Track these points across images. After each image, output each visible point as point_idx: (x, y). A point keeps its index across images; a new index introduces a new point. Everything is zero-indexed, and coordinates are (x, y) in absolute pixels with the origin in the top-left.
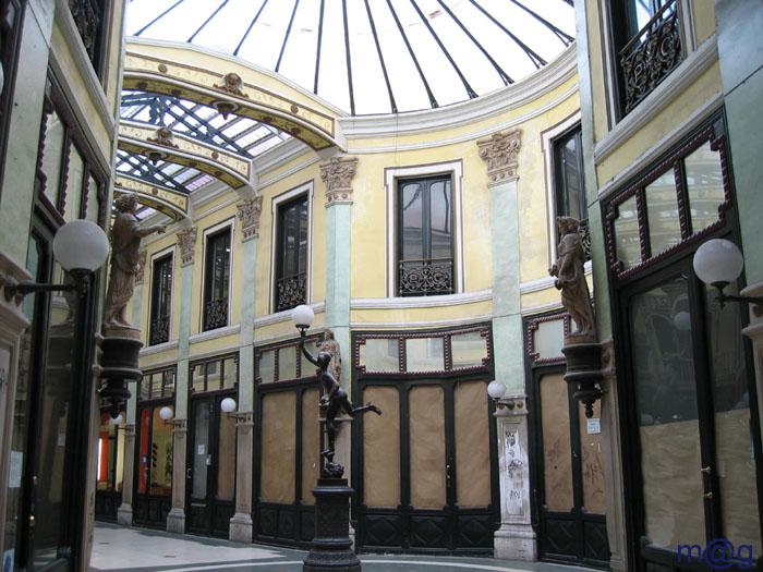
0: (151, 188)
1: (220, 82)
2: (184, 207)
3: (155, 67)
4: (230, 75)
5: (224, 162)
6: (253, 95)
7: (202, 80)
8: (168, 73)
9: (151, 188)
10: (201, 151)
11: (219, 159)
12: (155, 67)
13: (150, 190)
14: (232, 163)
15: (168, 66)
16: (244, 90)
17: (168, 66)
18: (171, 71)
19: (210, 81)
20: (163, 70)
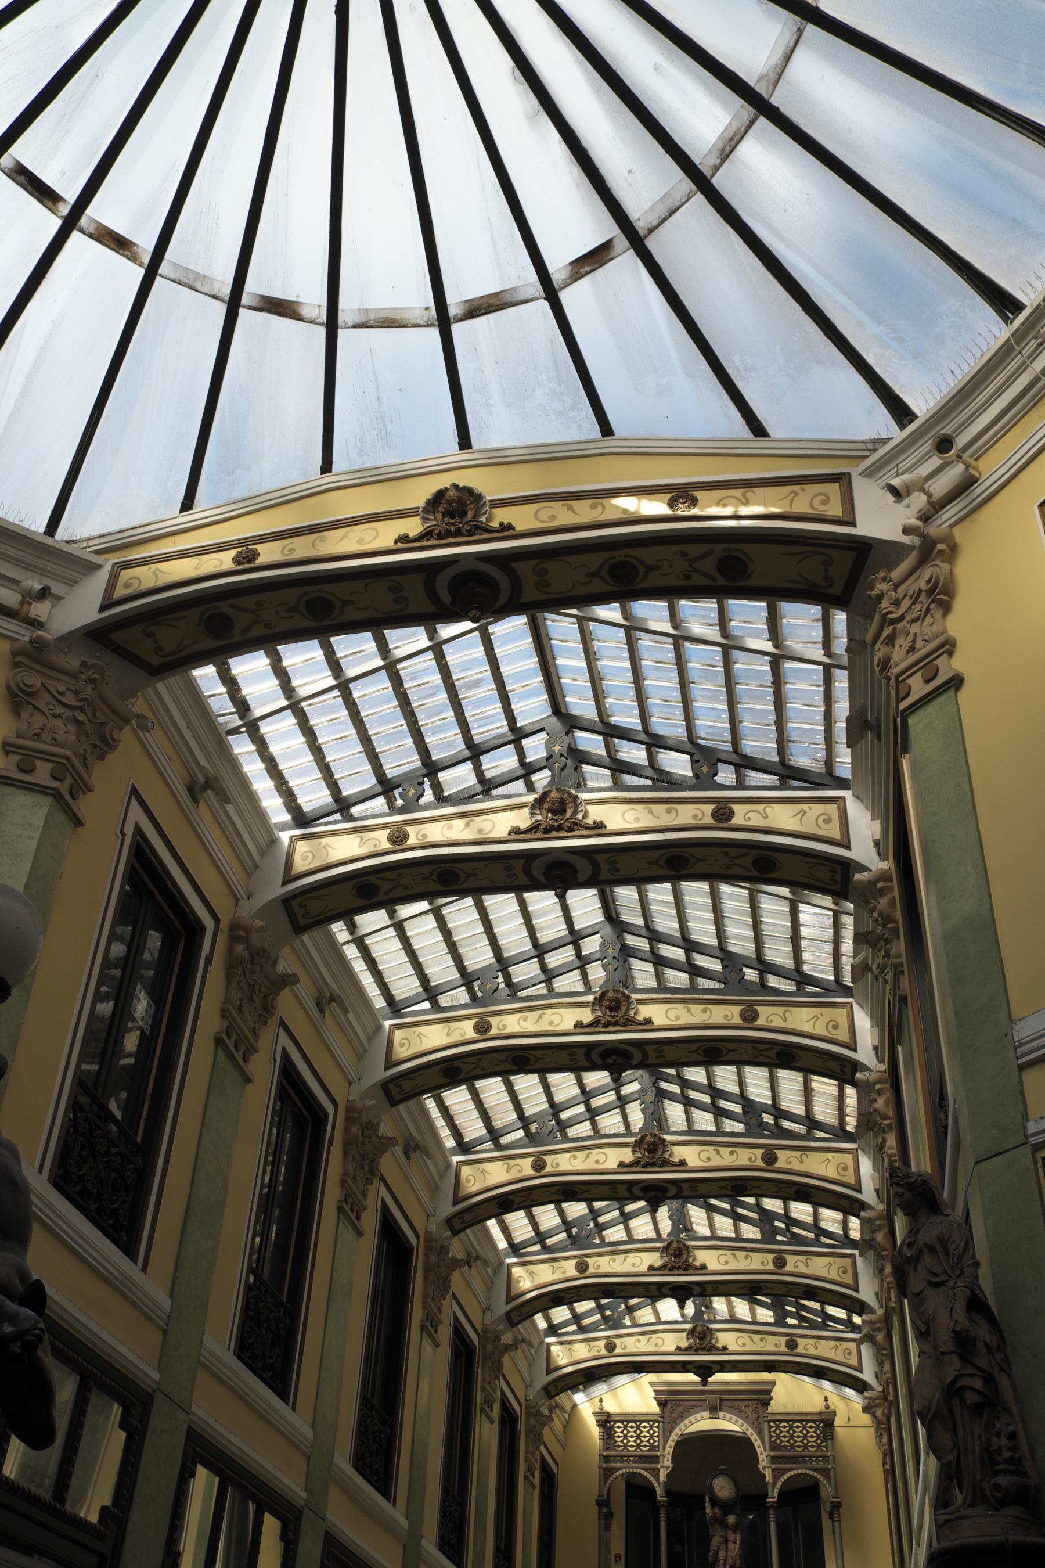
0: (736, 1010)
1: (413, 527)
2: (843, 1035)
3: (225, 560)
4: (440, 494)
5: (756, 821)
6: (522, 518)
7: (360, 541)
8: (260, 561)
9: (736, 1010)
10: (687, 817)
11: (738, 820)
12: (225, 560)
13: (732, 1014)
14: (783, 817)
15: (259, 548)
16: (502, 516)
17: (259, 548)
18: (268, 553)
19: (385, 535)
20: (247, 557)
